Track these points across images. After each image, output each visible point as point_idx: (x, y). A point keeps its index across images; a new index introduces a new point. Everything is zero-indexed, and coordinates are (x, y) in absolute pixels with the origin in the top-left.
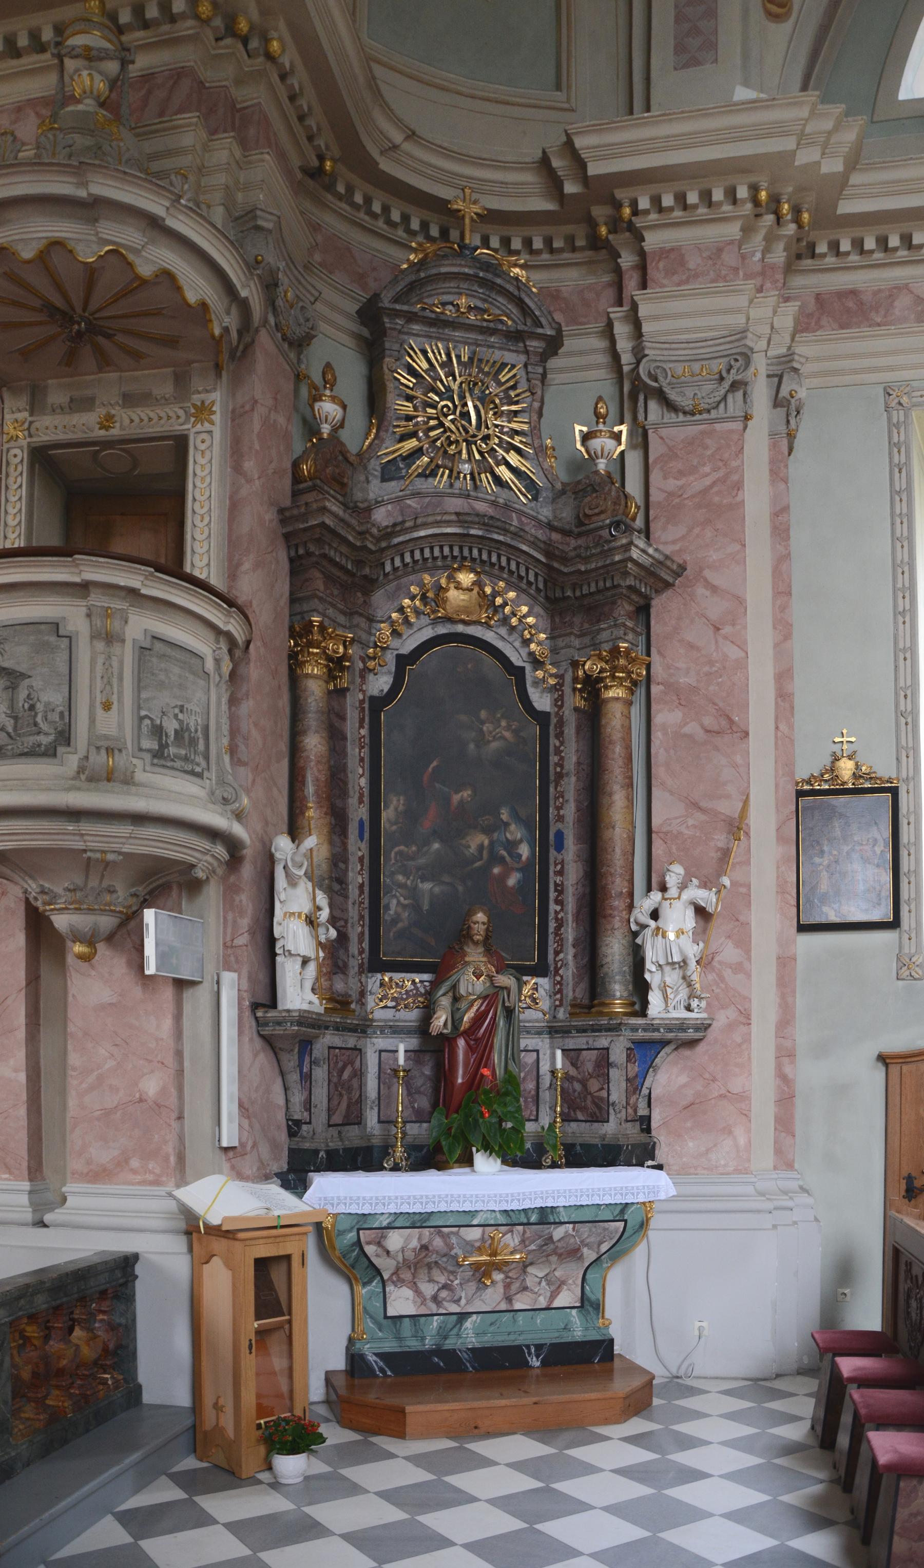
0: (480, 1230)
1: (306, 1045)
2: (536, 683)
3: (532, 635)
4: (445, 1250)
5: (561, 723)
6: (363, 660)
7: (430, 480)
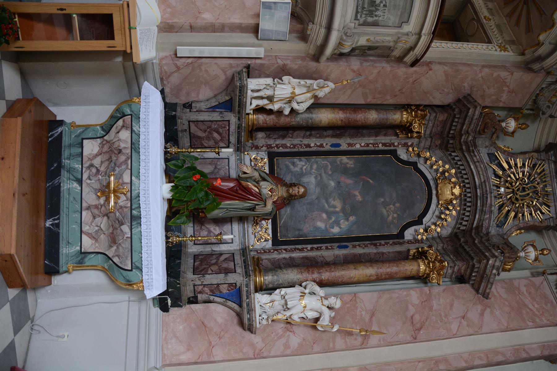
0: (129, 181)
1: (228, 106)
2: (416, 231)
3: (439, 225)
4: (118, 163)
5: (401, 244)
6: (412, 145)
7: (493, 175)
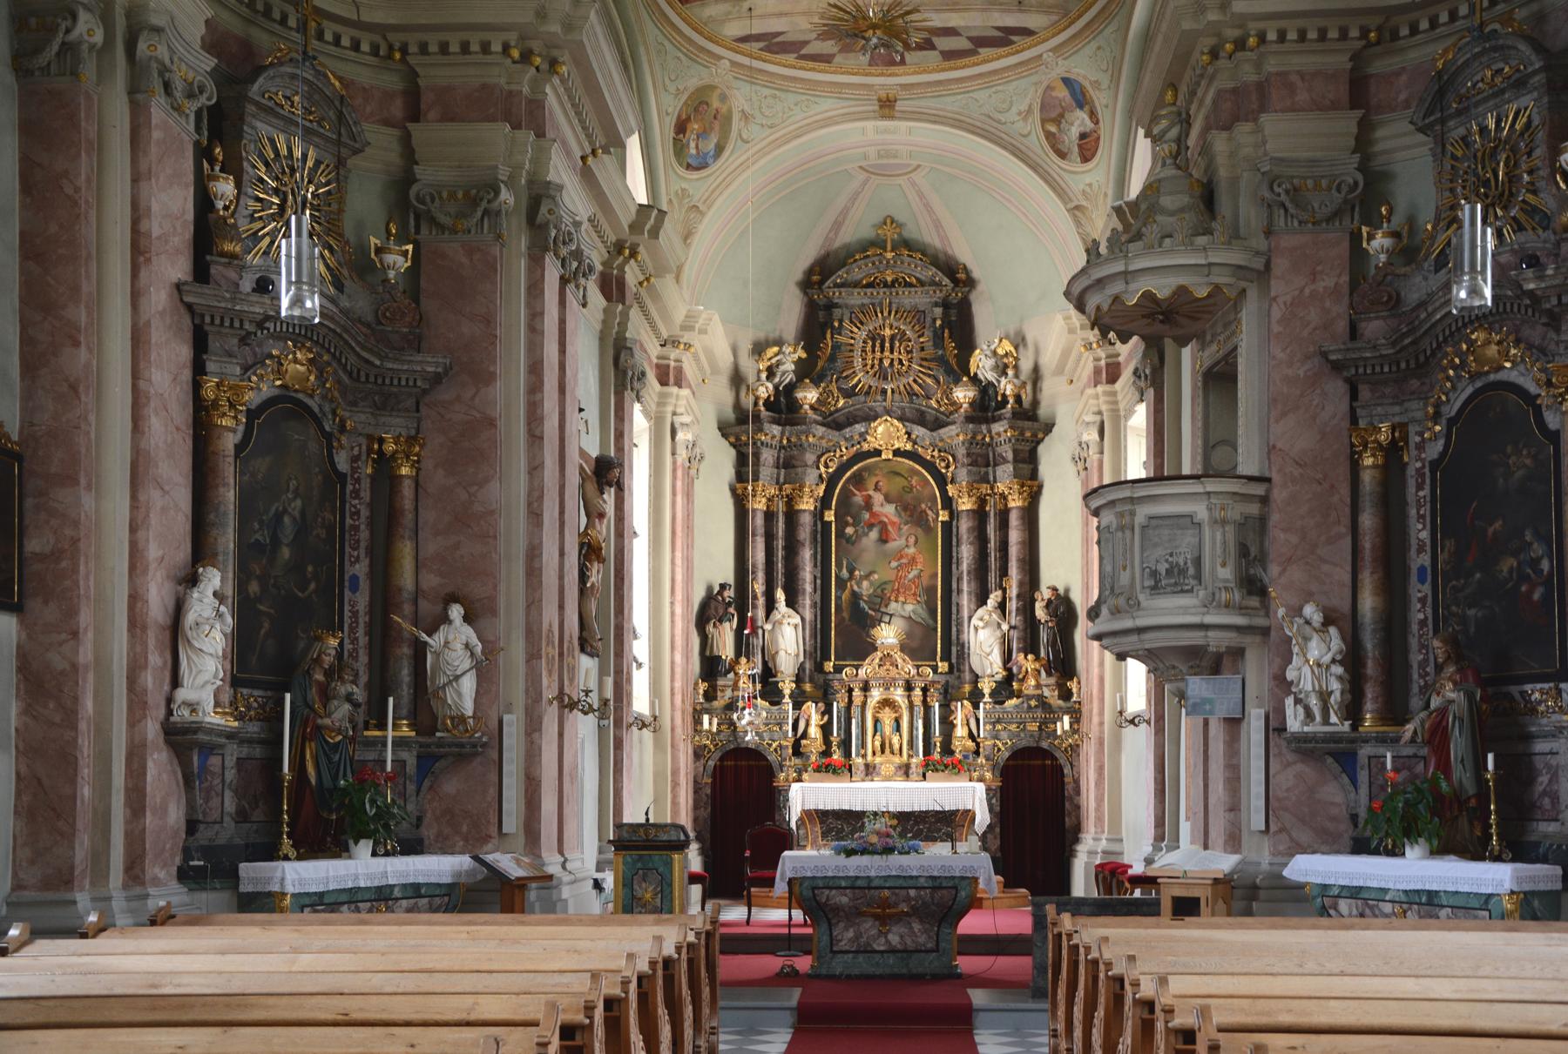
6: (1421, 434)
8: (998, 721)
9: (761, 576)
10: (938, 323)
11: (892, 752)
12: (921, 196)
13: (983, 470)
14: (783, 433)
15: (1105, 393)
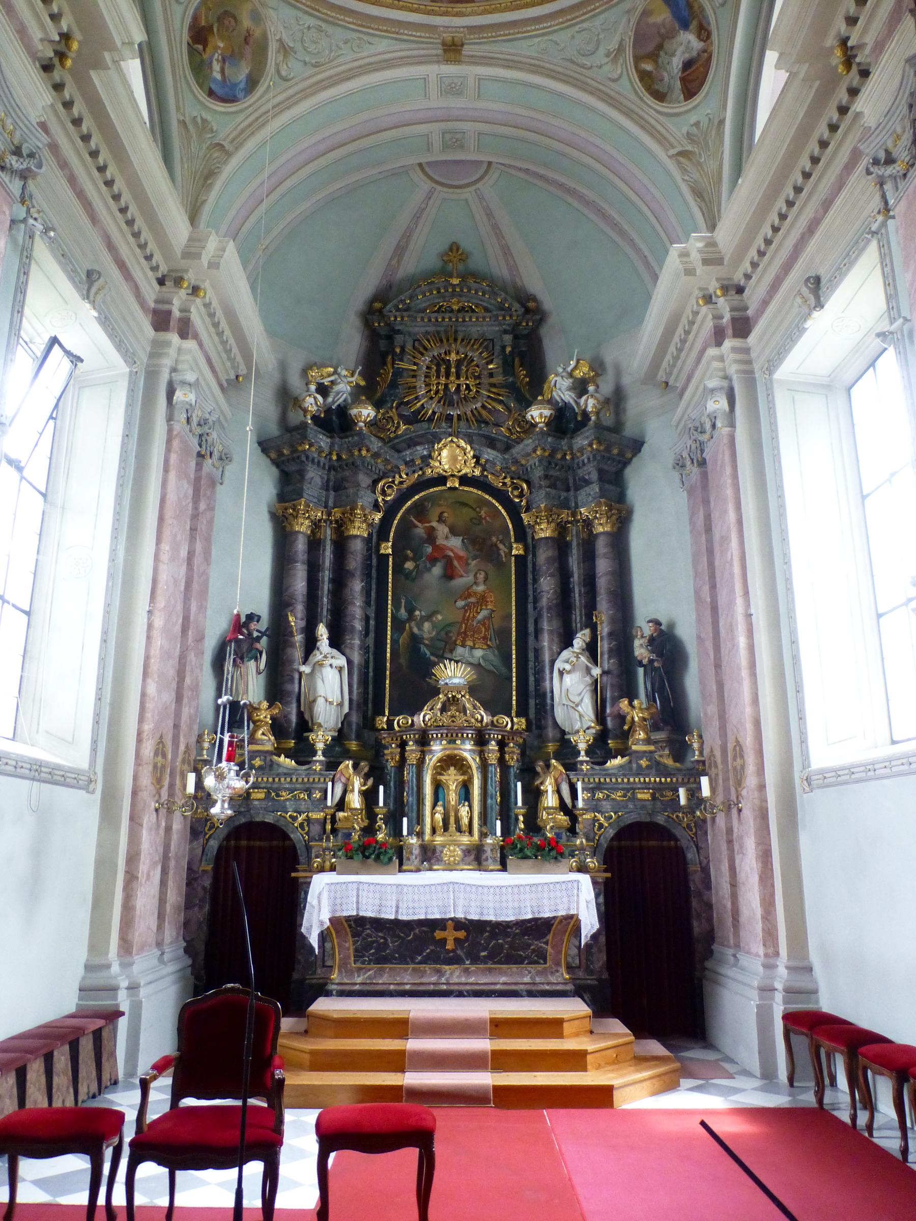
8: (599, 787)
9: (300, 608)
10: (508, 349)
11: (459, 829)
12: (490, 215)
13: (563, 495)
14: (332, 446)
15: (734, 350)
